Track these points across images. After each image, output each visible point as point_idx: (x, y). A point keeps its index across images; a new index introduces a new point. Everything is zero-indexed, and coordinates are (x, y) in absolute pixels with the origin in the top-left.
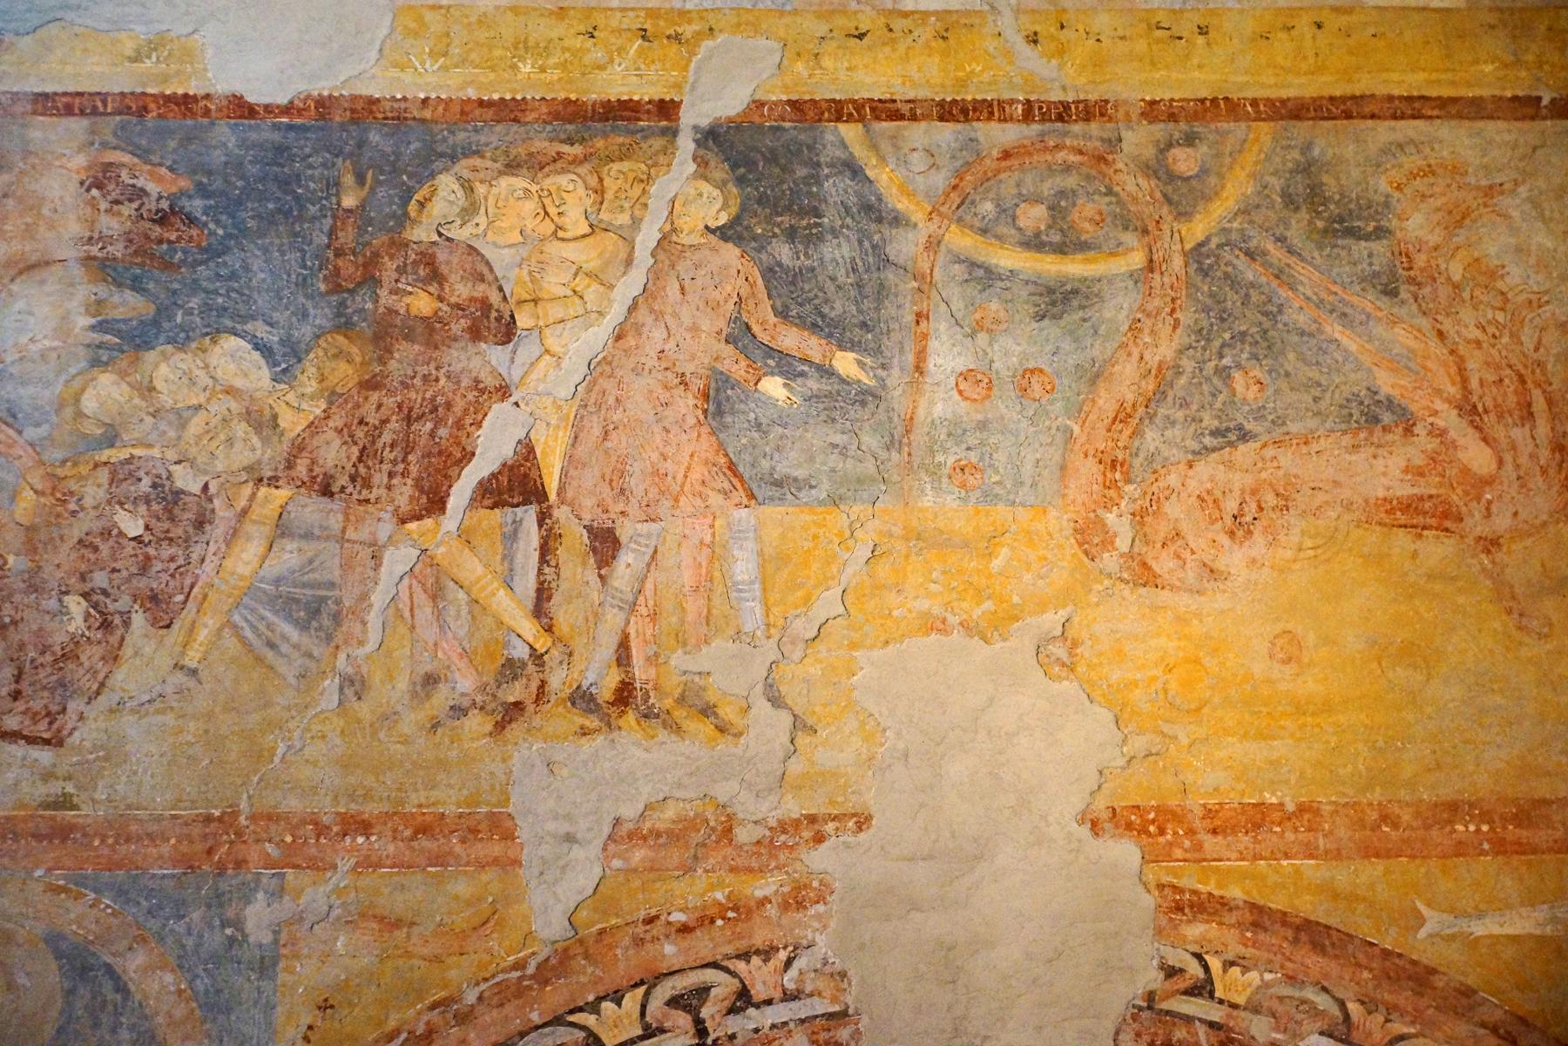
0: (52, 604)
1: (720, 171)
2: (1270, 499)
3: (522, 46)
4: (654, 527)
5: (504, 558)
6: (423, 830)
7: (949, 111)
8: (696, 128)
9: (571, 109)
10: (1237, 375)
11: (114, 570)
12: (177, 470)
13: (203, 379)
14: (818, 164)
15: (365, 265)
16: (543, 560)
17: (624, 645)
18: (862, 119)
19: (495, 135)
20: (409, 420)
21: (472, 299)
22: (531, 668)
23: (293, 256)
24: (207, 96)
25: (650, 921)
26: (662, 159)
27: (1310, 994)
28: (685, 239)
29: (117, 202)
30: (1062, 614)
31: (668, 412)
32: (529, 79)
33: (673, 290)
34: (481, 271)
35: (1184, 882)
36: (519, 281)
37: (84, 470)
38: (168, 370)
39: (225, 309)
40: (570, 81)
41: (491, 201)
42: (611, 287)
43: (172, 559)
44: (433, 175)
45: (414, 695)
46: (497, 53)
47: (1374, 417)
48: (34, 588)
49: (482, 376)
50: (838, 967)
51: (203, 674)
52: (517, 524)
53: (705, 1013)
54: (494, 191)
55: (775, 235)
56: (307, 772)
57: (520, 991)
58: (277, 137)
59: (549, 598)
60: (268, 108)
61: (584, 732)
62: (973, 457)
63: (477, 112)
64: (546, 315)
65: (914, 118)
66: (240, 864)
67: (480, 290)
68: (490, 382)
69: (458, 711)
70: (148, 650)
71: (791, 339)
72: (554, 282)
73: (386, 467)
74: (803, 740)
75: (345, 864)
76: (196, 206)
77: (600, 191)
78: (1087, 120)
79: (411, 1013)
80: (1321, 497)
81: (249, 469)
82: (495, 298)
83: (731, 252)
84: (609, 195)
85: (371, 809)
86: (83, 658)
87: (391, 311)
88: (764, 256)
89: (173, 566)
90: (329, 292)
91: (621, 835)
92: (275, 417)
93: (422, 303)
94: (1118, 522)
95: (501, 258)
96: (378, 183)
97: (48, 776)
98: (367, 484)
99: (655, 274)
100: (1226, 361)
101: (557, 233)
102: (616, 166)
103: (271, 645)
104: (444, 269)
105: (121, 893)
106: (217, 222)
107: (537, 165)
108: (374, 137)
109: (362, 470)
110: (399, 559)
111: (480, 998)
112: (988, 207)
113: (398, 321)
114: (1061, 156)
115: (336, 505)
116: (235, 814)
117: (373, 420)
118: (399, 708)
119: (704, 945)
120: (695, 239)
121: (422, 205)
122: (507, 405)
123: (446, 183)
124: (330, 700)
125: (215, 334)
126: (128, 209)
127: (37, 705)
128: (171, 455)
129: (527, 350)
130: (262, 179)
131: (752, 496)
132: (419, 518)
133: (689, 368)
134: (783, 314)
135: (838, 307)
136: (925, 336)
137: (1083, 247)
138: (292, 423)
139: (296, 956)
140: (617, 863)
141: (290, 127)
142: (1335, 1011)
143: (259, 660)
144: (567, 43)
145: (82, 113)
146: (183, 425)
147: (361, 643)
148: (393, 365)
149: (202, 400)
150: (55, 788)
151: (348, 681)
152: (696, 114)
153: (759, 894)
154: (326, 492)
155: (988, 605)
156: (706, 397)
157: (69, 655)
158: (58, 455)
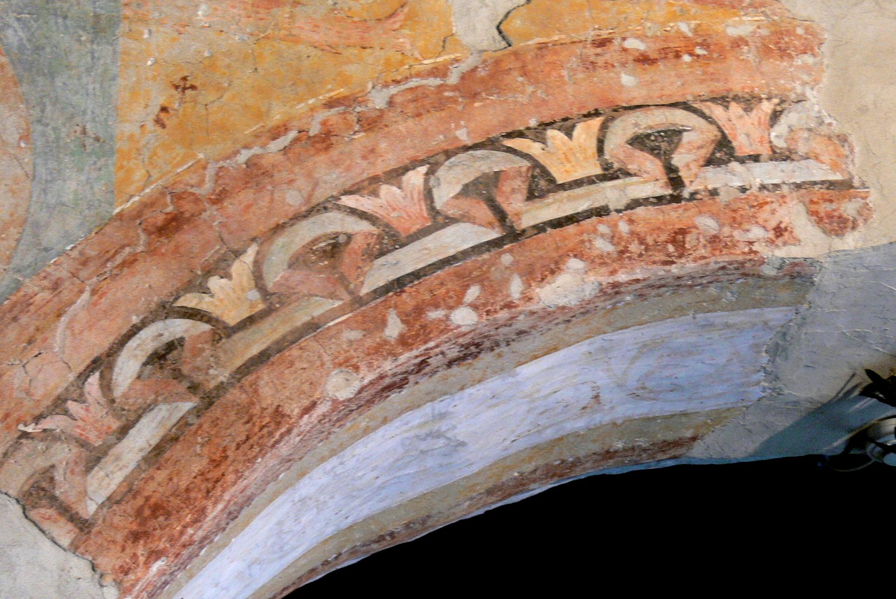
25: (602, 43)
50: (836, 128)
53: (678, 160)
79: (301, 108)
111: (391, 103)
119: (670, 81)
139: (144, 20)
153: (733, 32)
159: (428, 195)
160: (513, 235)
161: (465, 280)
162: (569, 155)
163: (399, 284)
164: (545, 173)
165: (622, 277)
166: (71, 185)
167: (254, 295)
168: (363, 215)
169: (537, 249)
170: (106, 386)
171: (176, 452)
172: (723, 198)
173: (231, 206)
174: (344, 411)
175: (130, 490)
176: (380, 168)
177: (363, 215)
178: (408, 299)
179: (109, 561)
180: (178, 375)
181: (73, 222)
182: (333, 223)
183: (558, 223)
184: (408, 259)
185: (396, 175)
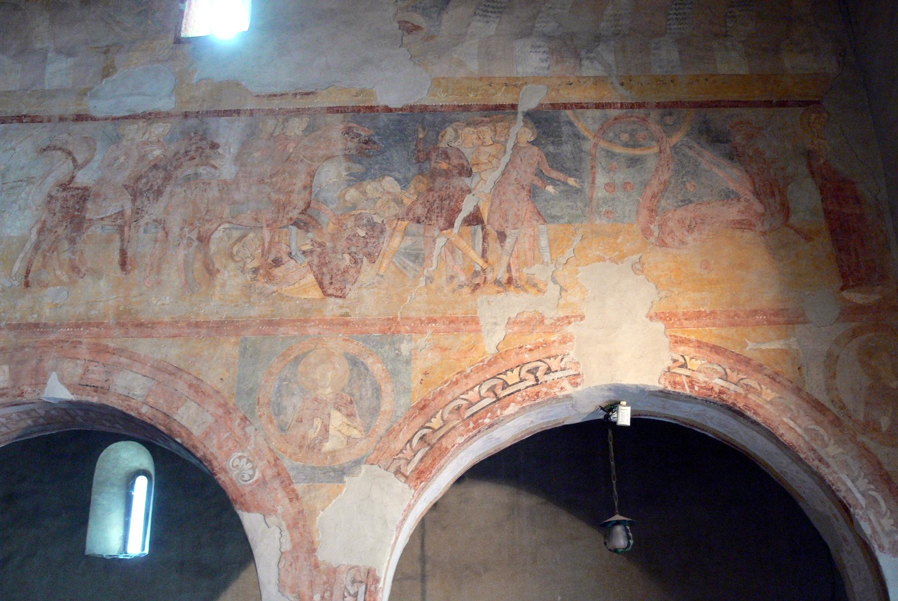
1: (531, 125)
2: (699, 221)
4: (517, 231)
6: (452, 322)
7: (598, 106)
13: (381, 190)
16: (484, 241)
17: (509, 266)
19: (463, 116)
25: (521, 348)
27: (715, 367)
28: (521, 145)
30: (639, 255)
32: (473, 99)
33: (518, 160)
34: (461, 156)
35: (678, 334)
37: (347, 217)
38: (370, 187)
47: (728, 196)
48: (334, 252)
52: (475, 231)
53: (538, 375)
60: (395, 109)
61: (498, 292)
62: (610, 209)
65: (588, 108)
66: (399, 332)
68: (465, 188)
69: (461, 286)
70: (369, 270)
71: (554, 174)
72: (483, 158)
74: (563, 294)
75: (429, 332)
76: (376, 139)
77: (495, 131)
80: (714, 220)
82: (466, 164)
83: (535, 149)
85: (436, 316)
87: (435, 168)
91: (510, 323)
93: (444, 166)
94: (654, 228)
95: (467, 152)
96: (429, 130)
97: (341, 307)
98: (430, 219)
99: (513, 155)
102: (500, 124)
103: (404, 268)
104: (450, 155)
105: (364, 341)
107: (476, 124)
108: (427, 117)
110: (441, 241)
112: (611, 134)
114: (632, 119)
115: (421, 226)
117: (431, 200)
119: (537, 355)
120: (523, 145)
121: (442, 136)
124: (422, 283)
125: (383, 176)
126: (356, 140)
127: (337, 286)
129: (476, 179)
131: (545, 221)
133: (525, 183)
134: (551, 167)
135: (568, 165)
136: (594, 173)
137: (640, 146)
138: (407, 202)
142: (723, 372)
143: (401, 272)
146: (375, 203)
147: (431, 266)
148: (436, 184)
150: (344, 310)
151: (427, 278)
152: (522, 108)
153: (552, 339)
154: (418, 222)
155: (617, 253)
157: (346, 271)
158: (339, 213)
160: (499, 399)
161: (487, 412)
162: (512, 377)
163: (472, 415)
164: (506, 383)
166: (402, 401)
170: (411, 446)
171: (425, 459)
173: (436, 401)
174: (463, 444)
175: (416, 468)
178: (474, 418)
179: (412, 484)
181: (403, 410)
183: (509, 395)
185: (472, 389)
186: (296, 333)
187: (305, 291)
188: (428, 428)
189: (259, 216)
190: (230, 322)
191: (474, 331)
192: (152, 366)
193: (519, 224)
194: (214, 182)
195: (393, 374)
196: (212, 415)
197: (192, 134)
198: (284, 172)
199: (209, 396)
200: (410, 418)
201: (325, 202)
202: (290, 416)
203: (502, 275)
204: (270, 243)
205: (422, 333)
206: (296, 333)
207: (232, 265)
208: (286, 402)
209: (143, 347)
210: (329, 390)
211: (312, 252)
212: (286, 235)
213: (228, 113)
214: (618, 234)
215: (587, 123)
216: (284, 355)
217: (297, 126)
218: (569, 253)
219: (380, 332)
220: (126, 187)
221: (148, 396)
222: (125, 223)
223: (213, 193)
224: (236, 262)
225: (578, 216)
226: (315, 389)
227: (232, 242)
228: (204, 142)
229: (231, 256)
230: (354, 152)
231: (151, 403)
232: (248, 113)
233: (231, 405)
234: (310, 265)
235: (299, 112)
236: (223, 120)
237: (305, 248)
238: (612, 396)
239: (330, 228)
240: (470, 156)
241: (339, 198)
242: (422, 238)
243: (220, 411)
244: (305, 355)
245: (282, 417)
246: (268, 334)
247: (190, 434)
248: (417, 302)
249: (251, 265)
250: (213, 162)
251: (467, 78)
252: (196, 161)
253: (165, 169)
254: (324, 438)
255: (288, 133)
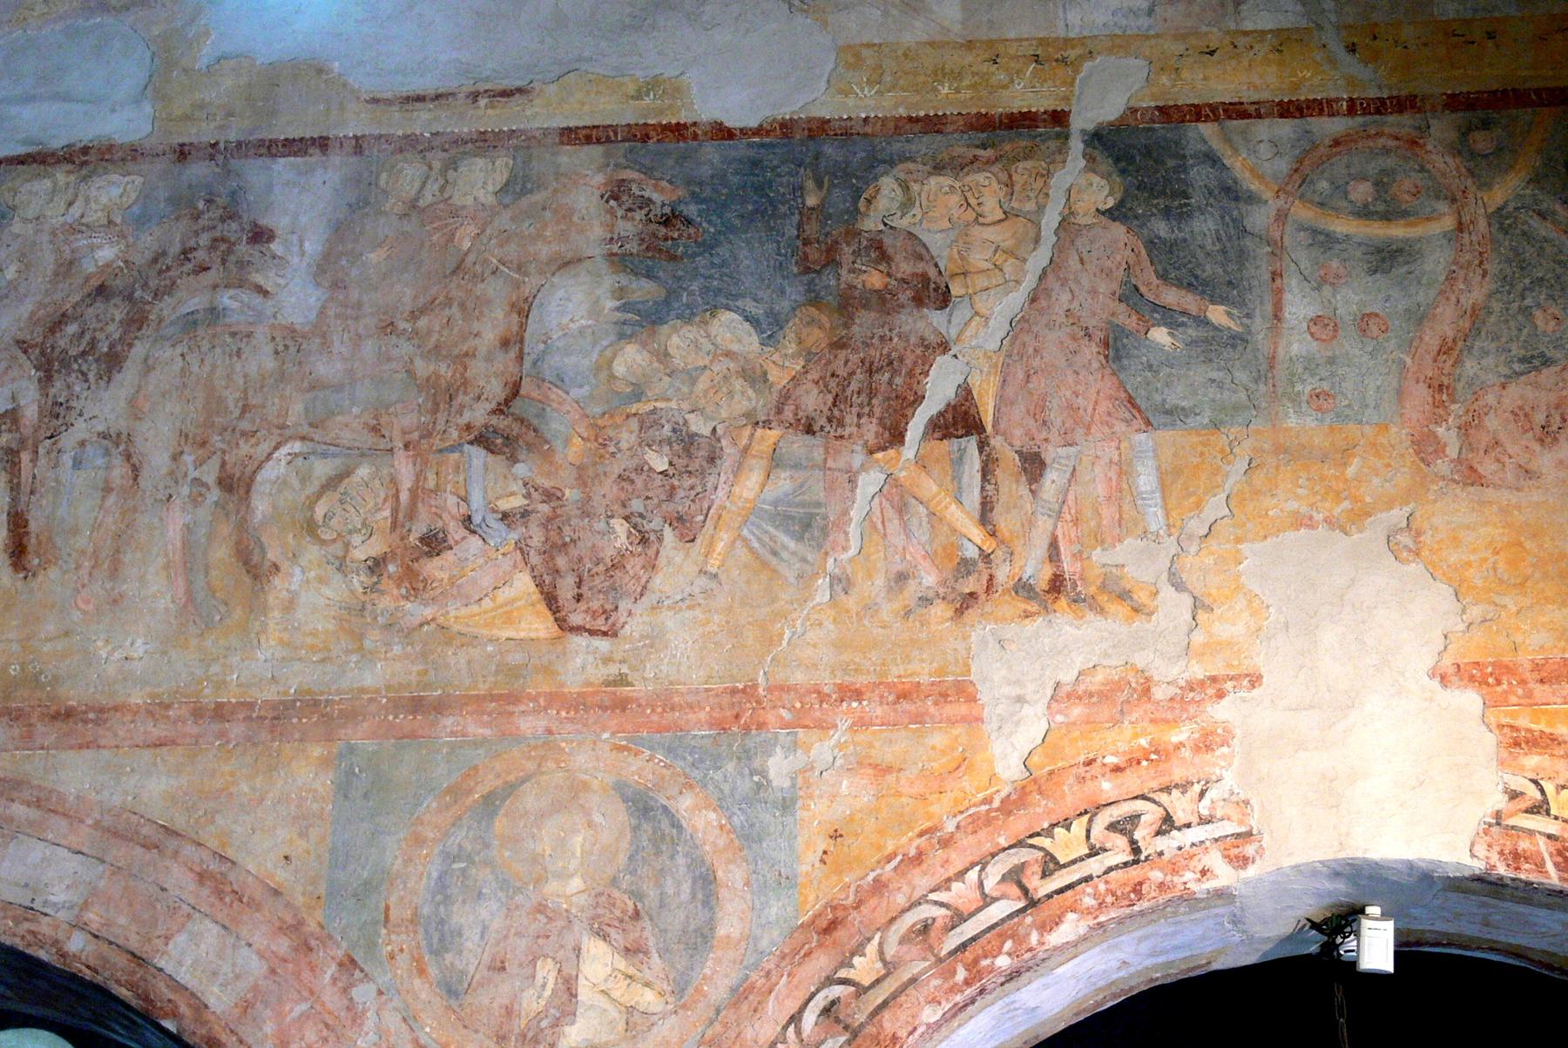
0: (601, 526)
1: (1106, 164)
3: (940, 74)
4: (1072, 450)
5: (953, 479)
6: (903, 696)
7: (1288, 110)
8: (1083, 132)
9: (983, 121)
10: (1538, 313)
11: (648, 498)
12: (691, 417)
13: (706, 345)
14: (1184, 157)
15: (828, 251)
16: (984, 476)
17: (1054, 545)
18: (1217, 119)
19: (925, 145)
20: (870, 372)
21: (915, 275)
22: (981, 565)
23: (770, 247)
24: (695, 124)
25: (1089, 763)
26: (1059, 158)
28: (1082, 220)
29: (630, 210)
30: (1407, 510)
31: (1077, 358)
32: (947, 99)
33: (1073, 262)
34: (920, 252)
35: (1523, 722)
36: (951, 259)
37: (618, 420)
38: (679, 340)
39: (720, 290)
40: (980, 99)
41: (924, 196)
42: (1025, 260)
43: (692, 488)
44: (876, 179)
45: (890, 590)
46: (921, 79)
48: (586, 514)
49: (926, 335)
51: (723, 577)
53: (1137, 835)
54: (926, 188)
55: (1153, 214)
56: (809, 652)
57: (988, 821)
58: (751, 153)
59: (992, 510)
61: (1027, 615)
62: (1326, 386)
63: (908, 127)
64: (974, 286)
65: (1259, 116)
66: (761, 726)
67: (920, 267)
68: (932, 339)
69: (925, 601)
70: (678, 559)
71: (1171, 297)
72: (979, 258)
73: (855, 410)
74: (1202, 616)
75: (843, 725)
76: (691, 210)
77: (1010, 185)
78: (1401, 112)
79: (904, 840)
81: (748, 415)
82: (932, 273)
83: (1118, 230)
84: (1016, 188)
85: (861, 680)
86: (628, 567)
87: (852, 287)
88: (1145, 231)
89: (693, 493)
90: (800, 274)
91: (1060, 696)
92: (765, 373)
93: (875, 280)
95: (937, 241)
96: (832, 185)
97: (607, 660)
98: (841, 424)
99: (1059, 248)
100: (1528, 302)
101: (978, 219)
102: (1021, 165)
103: (775, 553)
104: (890, 251)
105: (670, 750)
106: (710, 222)
107: (959, 167)
108: (828, 150)
109: (836, 412)
110: (869, 482)
111: (958, 827)
112: (1324, 185)
113: (857, 293)
114: (1381, 141)
115: (817, 441)
116: (755, 686)
117: (842, 372)
118: (879, 600)
119: (1133, 781)
120: (1088, 220)
121: (869, 201)
122: (947, 357)
123: (888, 184)
124: (822, 596)
125: (713, 310)
126: (639, 215)
127: (595, 605)
128: (686, 406)
129: (961, 313)
130: (744, 187)
131: (1148, 423)
132: (884, 449)
133: (1092, 323)
134: (1163, 276)
135: (1209, 270)
136: (1280, 291)
137: (1405, 214)
138: (778, 378)
139: (811, 797)
140: (1059, 718)
141: (762, 145)
143: (765, 565)
144: (974, 69)
145: (598, 141)
146: (694, 381)
147: (845, 549)
148: (855, 329)
149: (707, 362)
150: (613, 669)
151: (835, 580)
152: (1082, 121)
153: (1175, 739)
154: (809, 430)
155: (1346, 504)
156: (1107, 345)
157: (617, 565)
158: (598, 410)
159: (981, 885)
160: (1033, 903)
161: (1003, 938)
162: (1067, 844)
163: (963, 946)
164: (1053, 858)
165: (1102, 919)
166: (773, 911)
167: (879, 965)
168: (942, 905)
169: (1045, 912)
170: (798, 1032)
172: (1166, 857)
174: (937, 1026)
176: (952, 871)
177: (942, 905)
178: (968, 955)
180: (837, 1020)
181: (776, 933)
182: (926, 912)
183: (1061, 891)
184: (969, 929)
185: (961, 875)
186: (487, 732)
187: (509, 620)
188: (844, 982)
189: (383, 420)
190: (310, 704)
191: (964, 719)
192: (97, 825)
193: (1080, 431)
194: (261, 333)
195: (748, 838)
196: (261, 955)
197: (201, 205)
198: (449, 302)
199: (254, 905)
200: (796, 955)
201: (560, 381)
202: (471, 956)
203: (1035, 568)
204: (414, 492)
205: (824, 726)
206: (487, 732)
207: (312, 552)
208: (461, 916)
209: (75, 774)
210: (576, 884)
211: (525, 514)
212: (457, 468)
213: (294, 147)
214: (1346, 453)
215: (1257, 158)
216: (456, 792)
217: (480, 181)
218: (1215, 507)
219: (711, 726)
220: (23, 345)
221: (86, 906)
222: (22, 441)
223: (260, 359)
224: (323, 542)
225: (1237, 408)
226: (539, 881)
227: (311, 489)
228: (234, 226)
229: (311, 528)
230: (633, 247)
231: (94, 927)
232: (349, 146)
233: (312, 926)
234: (522, 548)
235: (485, 142)
236: (283, 167)
237: (504, 505)
238: (1341, 891)
239: (574, 450)
240: (945, 254)
241: (598, 369)
242: (818, 474)
243: (283, 945)
244: (511, 789)
245: (449, 957)
246: (413, 735)
247: (200, 1007)
248: (810, 646)
249: (363, 550)
250: (258, 278)
251: (932, 44)
252: (211, 276)
253: (130, 298)
254: (564, 1014)
255: (457, 200)
